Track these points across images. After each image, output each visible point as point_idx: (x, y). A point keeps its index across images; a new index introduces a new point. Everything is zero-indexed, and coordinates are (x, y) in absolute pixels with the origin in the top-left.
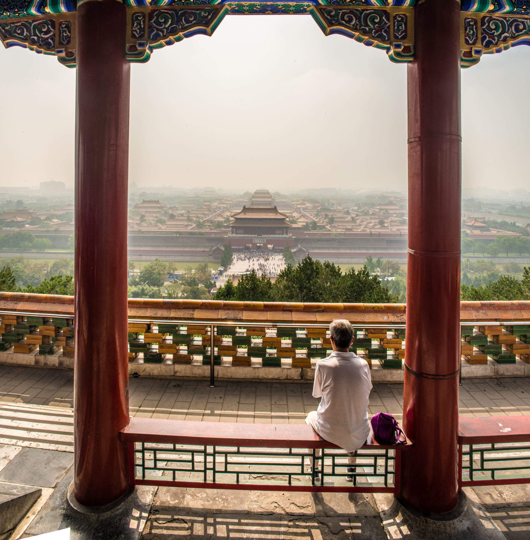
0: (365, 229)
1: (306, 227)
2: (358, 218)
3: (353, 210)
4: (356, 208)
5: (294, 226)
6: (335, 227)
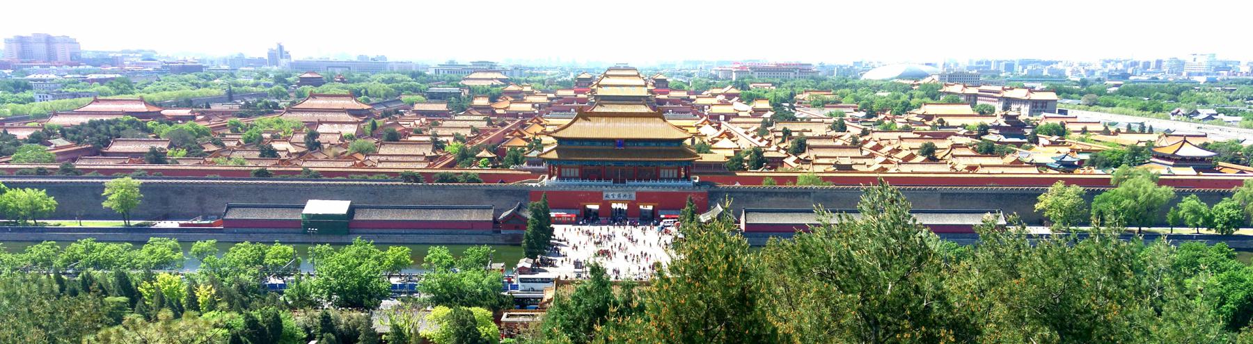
0: (885, 166)
1: (737, 162)
2: (867, 138)
3: (855, 120)
4: (863, 114)
5: (706, 158)
6: (806, 161)
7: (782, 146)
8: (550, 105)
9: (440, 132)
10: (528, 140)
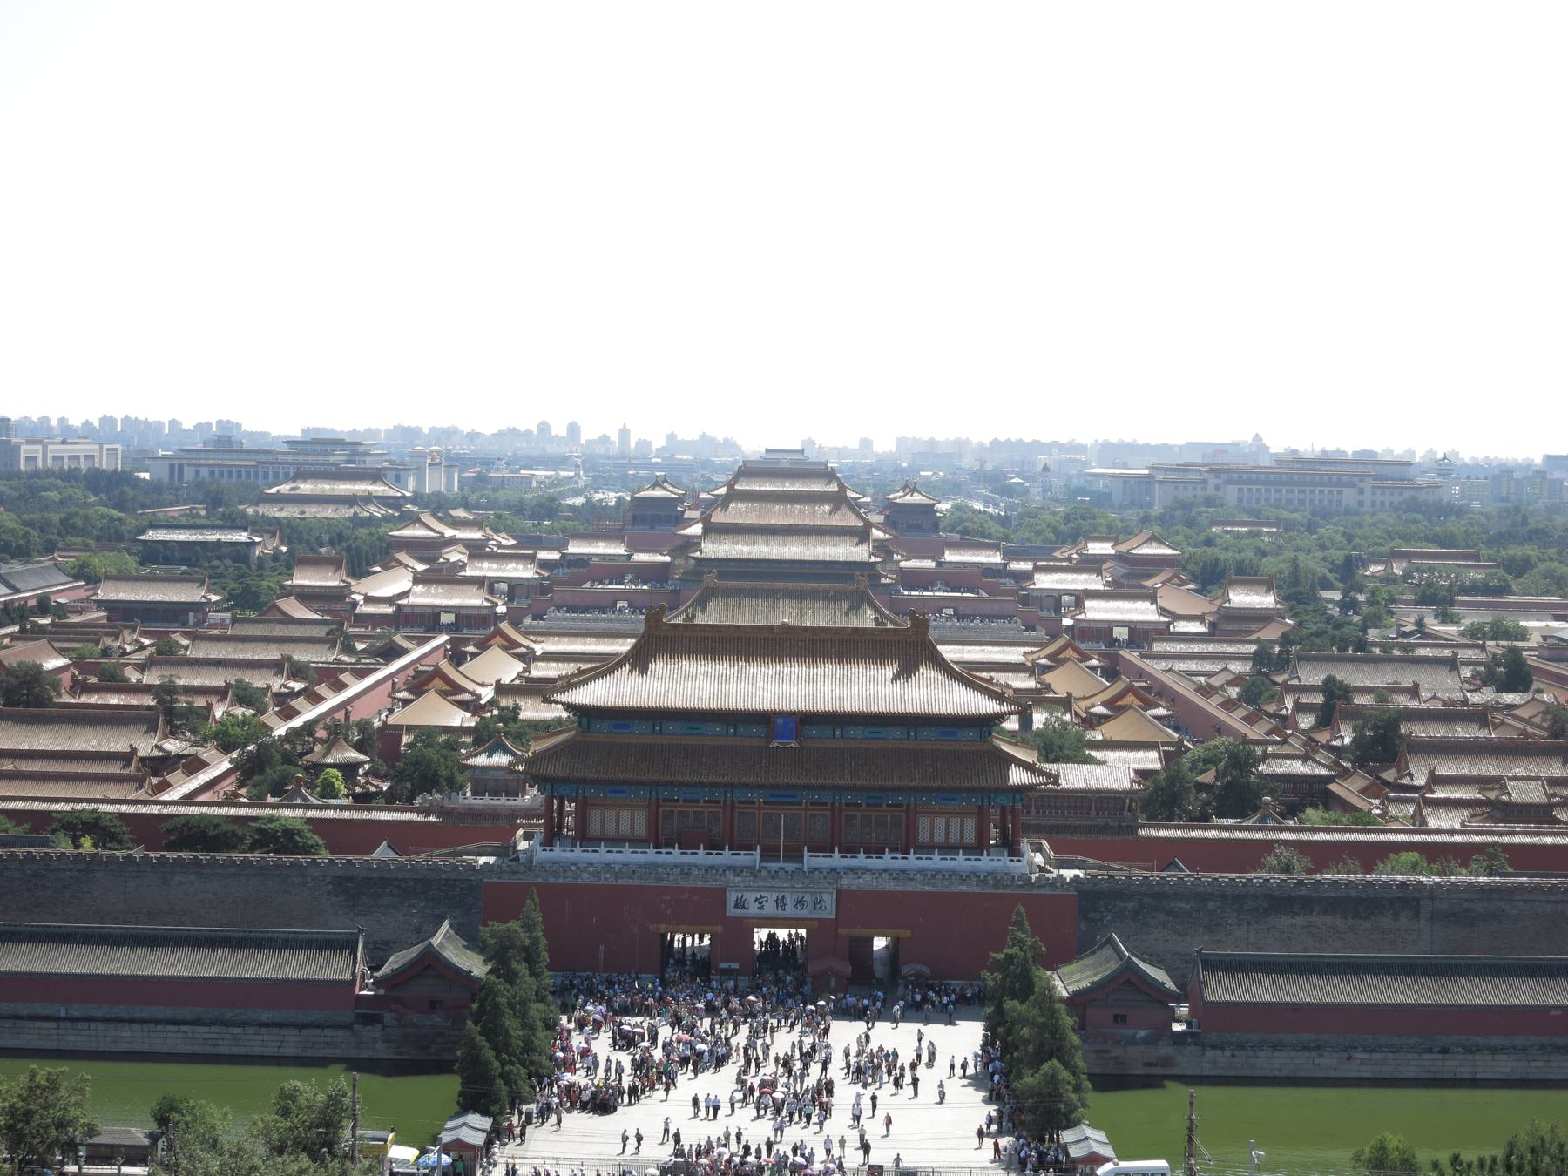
5: (1074, 777)
7: (1323, 737)
8: (544, 591)
9: (186, 679)
10: (472, 706)
